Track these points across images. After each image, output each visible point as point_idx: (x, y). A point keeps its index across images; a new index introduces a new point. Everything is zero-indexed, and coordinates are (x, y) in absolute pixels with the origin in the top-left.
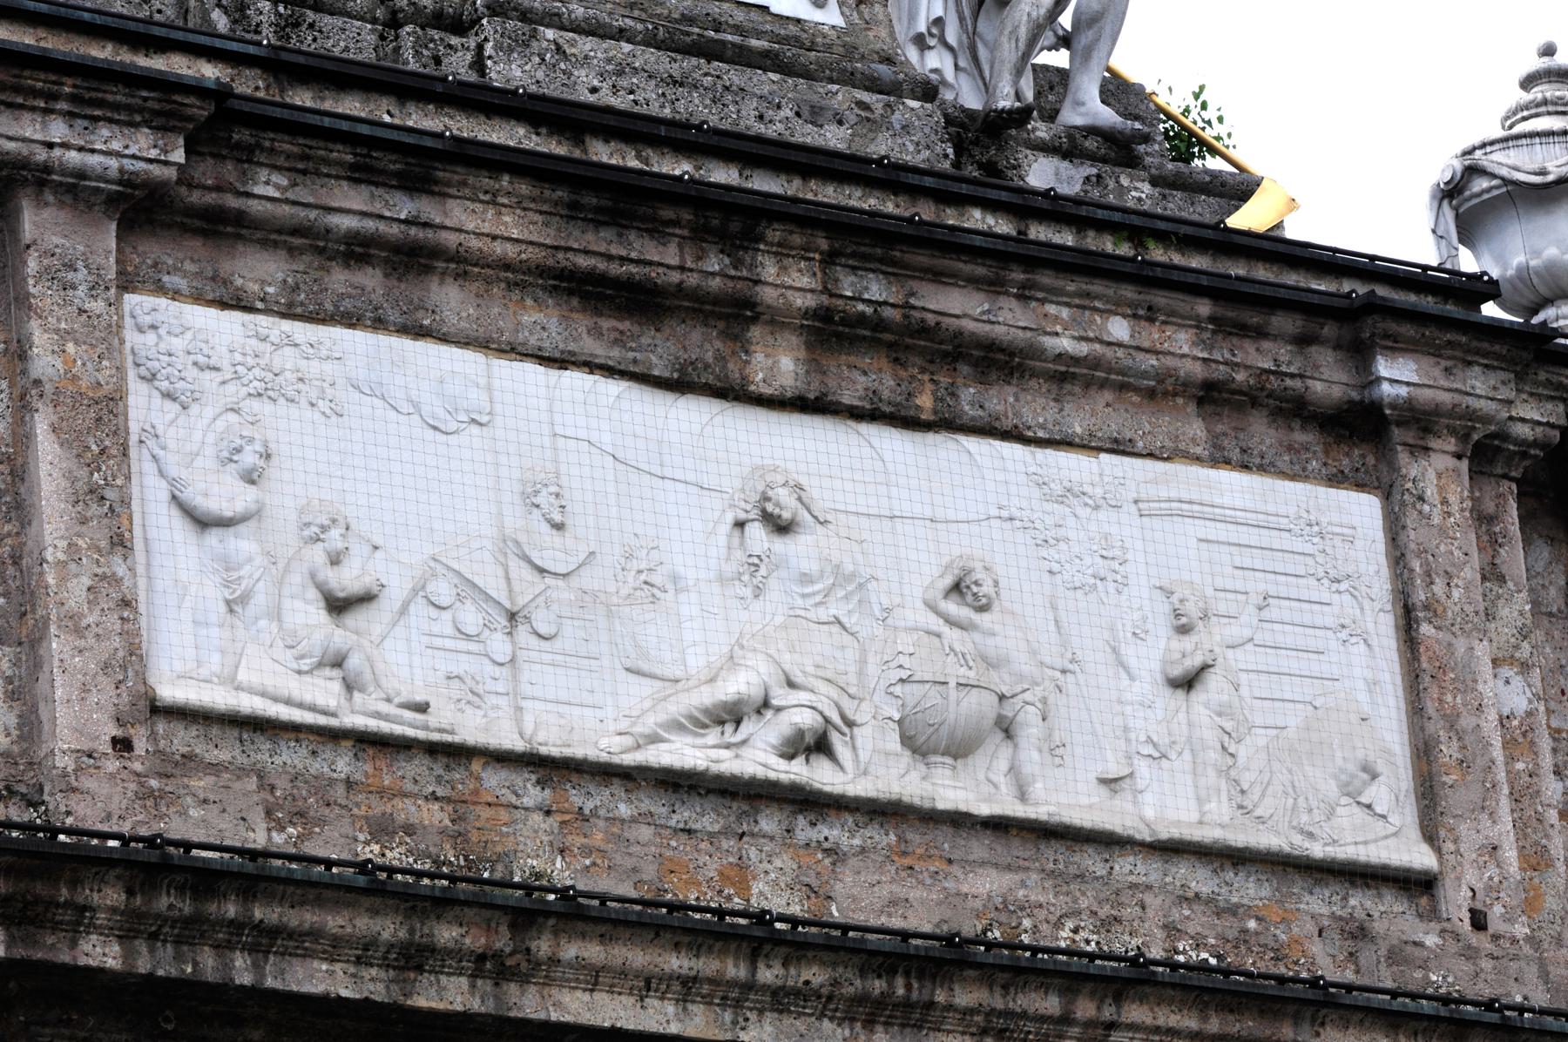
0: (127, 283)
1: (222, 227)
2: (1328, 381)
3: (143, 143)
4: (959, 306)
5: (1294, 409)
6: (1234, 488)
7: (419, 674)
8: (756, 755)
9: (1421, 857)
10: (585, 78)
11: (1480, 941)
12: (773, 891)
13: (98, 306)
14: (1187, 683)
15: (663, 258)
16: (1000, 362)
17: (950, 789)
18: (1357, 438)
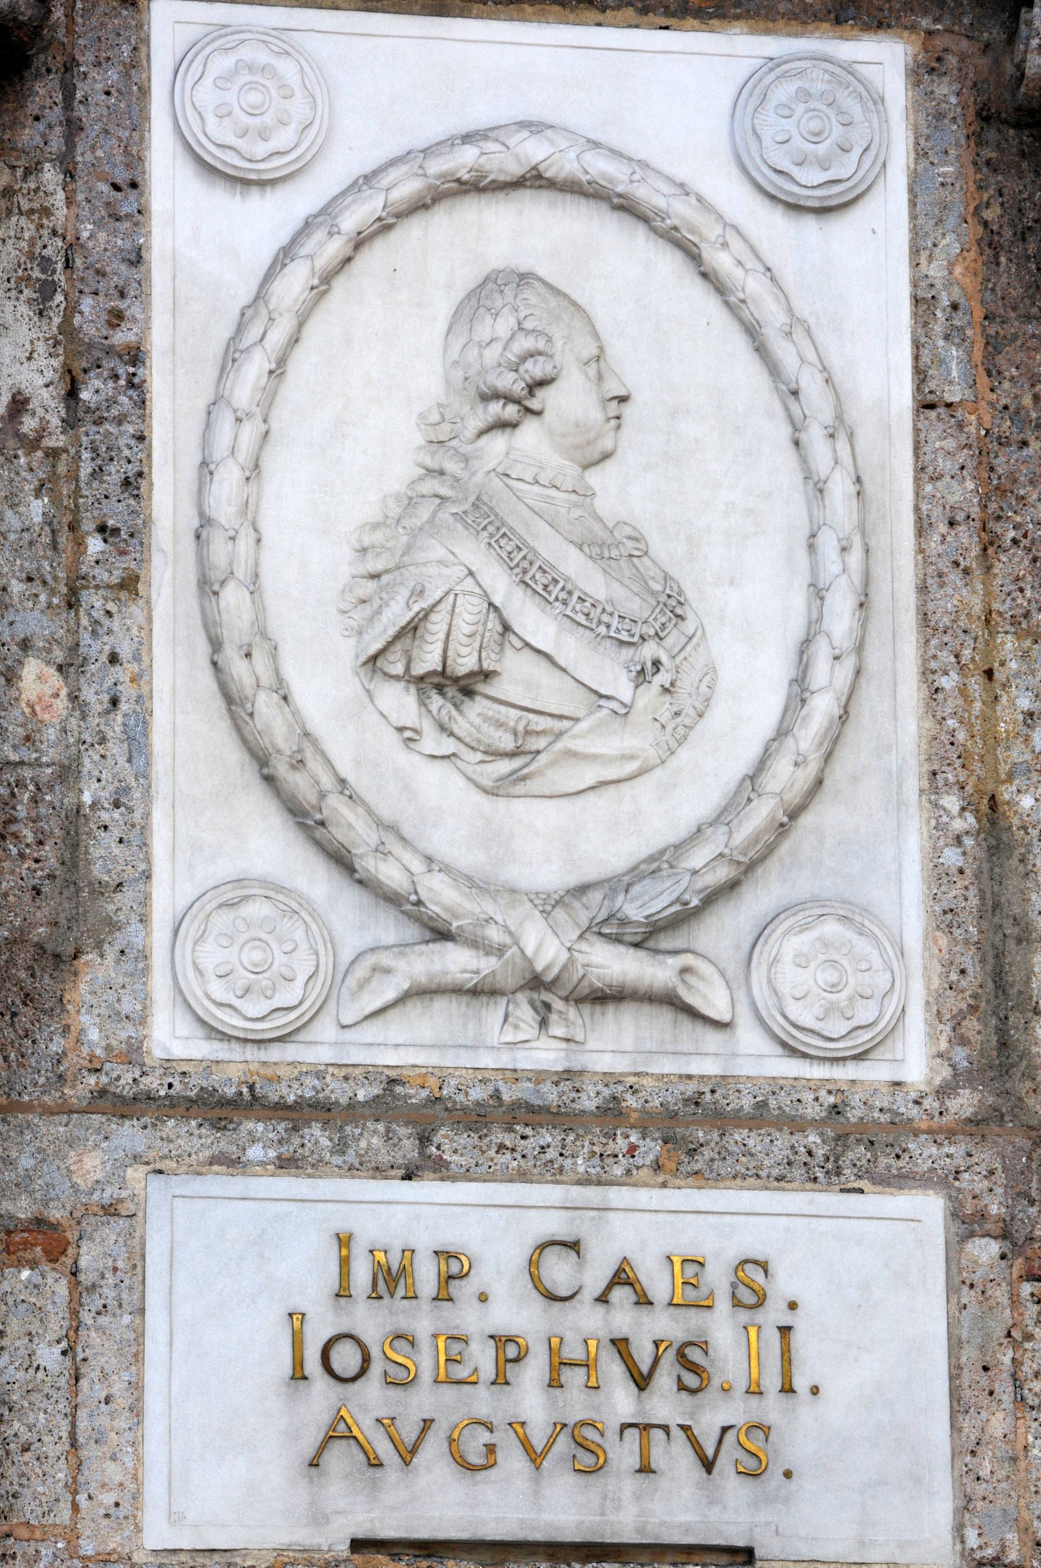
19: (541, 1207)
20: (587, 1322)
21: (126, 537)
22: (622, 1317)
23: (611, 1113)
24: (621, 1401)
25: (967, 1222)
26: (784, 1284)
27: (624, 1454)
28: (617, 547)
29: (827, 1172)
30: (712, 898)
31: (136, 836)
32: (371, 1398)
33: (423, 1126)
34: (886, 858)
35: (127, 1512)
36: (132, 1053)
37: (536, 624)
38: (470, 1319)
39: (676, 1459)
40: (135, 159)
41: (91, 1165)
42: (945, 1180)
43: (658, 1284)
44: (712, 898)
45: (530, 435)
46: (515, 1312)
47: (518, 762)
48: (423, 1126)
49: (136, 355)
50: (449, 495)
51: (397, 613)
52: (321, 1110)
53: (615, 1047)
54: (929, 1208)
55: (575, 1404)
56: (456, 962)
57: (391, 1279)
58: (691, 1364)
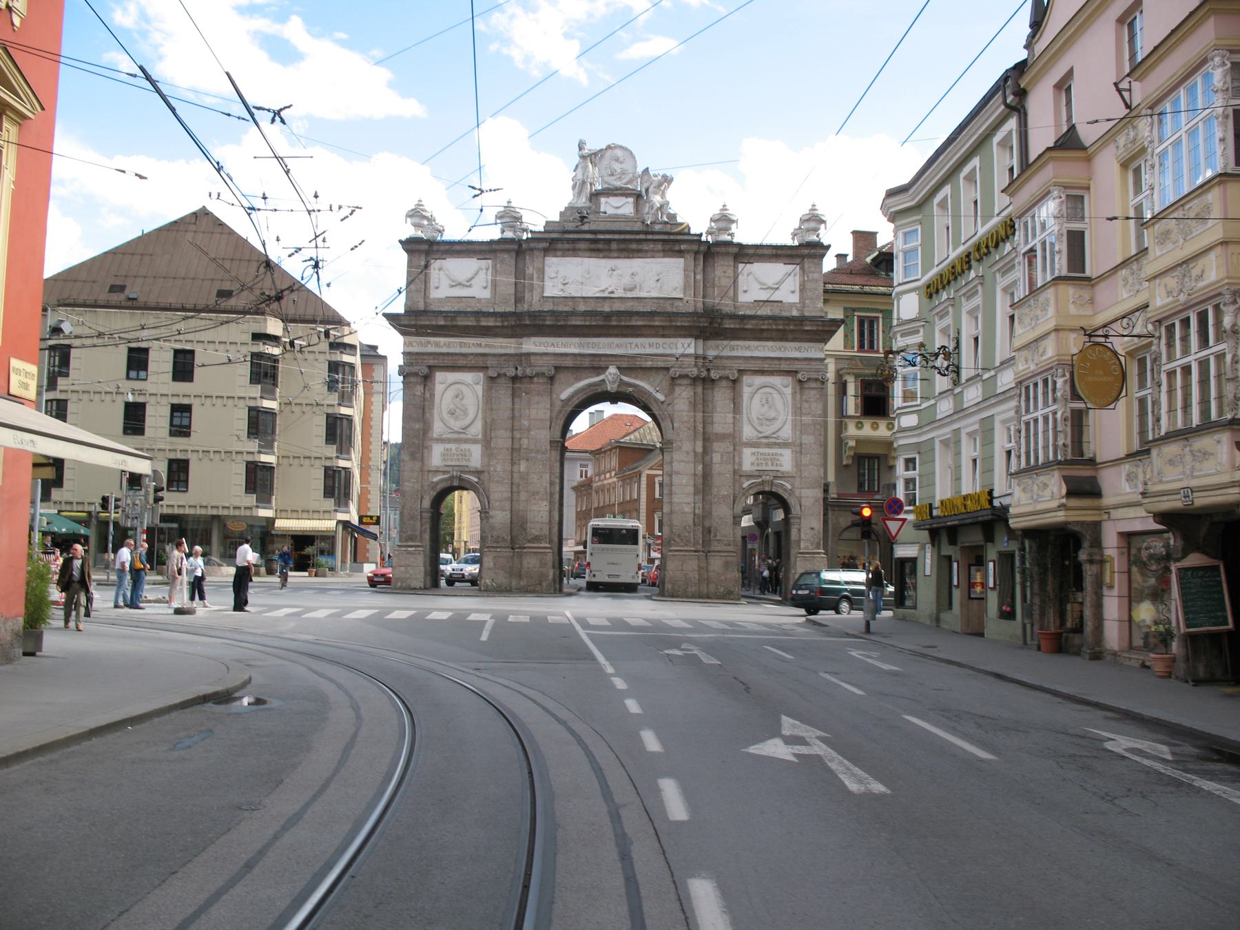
1: (556, 250)
2: (677, 248)
4: (634, 246)
5: (673, 251)
6: (666, 260)
7: (573, 291)
8: (606, 295)
9: (681, 296)
12: (607, 309)
15: (600, 246)
16: (639, 251)
17: (629, 295)
18: (680, 253)
47: (457, 419)
48: (449, 441)
53: (462, 436)
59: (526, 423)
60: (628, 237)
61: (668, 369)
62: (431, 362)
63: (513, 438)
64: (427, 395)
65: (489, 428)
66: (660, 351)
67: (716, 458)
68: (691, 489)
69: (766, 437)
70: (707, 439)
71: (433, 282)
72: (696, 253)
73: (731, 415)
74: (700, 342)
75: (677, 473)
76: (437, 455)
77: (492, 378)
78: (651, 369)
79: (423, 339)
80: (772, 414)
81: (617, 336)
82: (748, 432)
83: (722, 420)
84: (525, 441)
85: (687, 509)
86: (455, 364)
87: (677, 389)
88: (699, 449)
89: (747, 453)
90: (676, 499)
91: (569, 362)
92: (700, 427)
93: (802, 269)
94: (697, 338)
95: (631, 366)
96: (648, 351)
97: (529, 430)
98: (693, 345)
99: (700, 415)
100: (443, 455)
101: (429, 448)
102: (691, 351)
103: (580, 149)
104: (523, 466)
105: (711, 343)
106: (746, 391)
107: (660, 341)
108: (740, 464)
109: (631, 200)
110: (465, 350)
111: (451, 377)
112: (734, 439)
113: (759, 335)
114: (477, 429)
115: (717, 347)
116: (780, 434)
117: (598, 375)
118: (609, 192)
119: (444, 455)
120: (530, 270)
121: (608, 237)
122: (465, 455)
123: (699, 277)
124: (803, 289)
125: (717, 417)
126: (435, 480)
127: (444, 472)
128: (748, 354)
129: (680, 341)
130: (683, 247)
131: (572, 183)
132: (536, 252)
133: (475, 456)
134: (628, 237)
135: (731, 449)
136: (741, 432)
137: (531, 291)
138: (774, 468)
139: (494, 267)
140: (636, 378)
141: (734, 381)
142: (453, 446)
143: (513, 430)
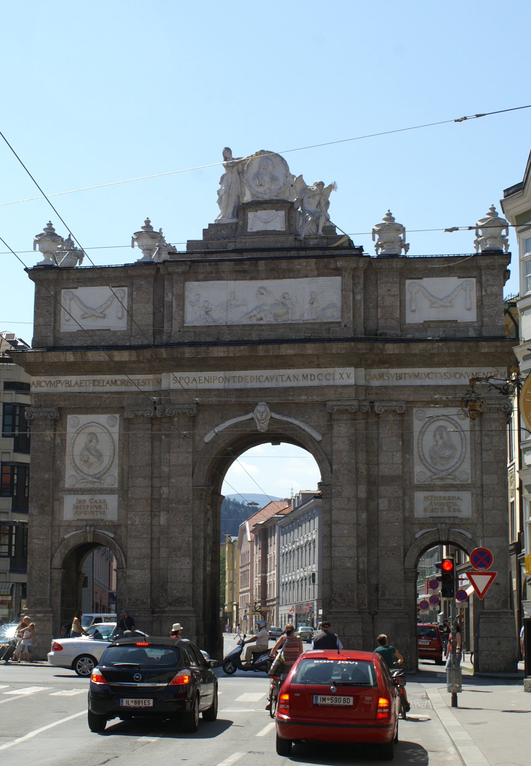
0: (185, 280)
2: (332, 266)
3: (184, 267)
4: (284, 264)
8: (254, 322)
10: (247, 244)
11: (346, 328)
13: (181, 285)
14: (312, 303)
16: (290, 270)
18: (337, 272)
19: (90, 497)
20: (93, 504)
21: (65, 452)
22: (96, 504)
23: (96, 490)
24: (95, 510)
25: (119, 497)
26: (107, 501)
27: (95, 513)
28: (97, 451)
29: (109, 494)
30: (103, 475)
31: (65, 473)
32: (78, 510)
33: (83, 491)
34: (115, 471)
35: (62, 518)
36: (64, 487)
37: (91, 457)
38: (86, 504)
39: (99, 513)
40: (66, 426)
41: (61, 495)
42: (118, 494)
43: (98, 501)
44: (103, 475)
45: (92, 443)
46: (88, 504)
48: (83, 491)
49: (66, 440)
50: (87, 448)
51: (82, 456)
52: (76, 490)
53: (96, 486)
54: (117, 496)
55: (92, 510)
56: (85, 480)
57: (80, 501)
58: (100, 507)
59: (166, 469)
60: (277, 254)
61: (324, 404)
62: (62, 404)
63: (152, 487)
64: (58, 440)
65: (126, 475)
66: (316, 383)
67: (383, 504)
68: (353, 541)
69: (442, 479)
70: (373, 482)
71: (63, 316)
72: (355, 269)
73: (399, 455)
74: (362, 371)
75: (337, 523)
76: (69, 509)
77: (129, 419)
78: (305, 404)
79: (53, 379)
80: (448, 453)
81: (266, 368)
82: (420, 473)
83: (389, 462)
84: (165, 490)
85: (349, 565)
86: (87, 404)
87: (335, 427)
88: (363, 495)
89: (419, 496)
90: (336, 554)
91: (214, 400)
92: (363, 469)
93: (480, 282)
94: (357, 366)
95: (283, 400)
96: (302, 383)
97: (169, 477)
98: (352, 375)
99: (362, 457)
100: (76, 507)
101: (60, 501)
102: (352, 382)
103: (226, 159)
104: (163, 519)
105: (375, 371)
106: (417, 425)
107: (315, 371)
108: (412, 510)
109: (282, 214)
110: (98, 389)
111: (84, 419)
112: (404, 483)
113: (429, 361)
114: (112, 480)
115: (381, 376)
116: (457, 473)
117: (246, 413)
118: (258, 204)
119: (77, 508)
120: (168, 298)
121: (255, 255)
122: (100, 507)
123: (359, 297)
124: (480, 306)
125: (383, 459)
126: (66, 537)
127: (77, 528)
128: (418, 382)
129: (339, 370)
130: (339, 264)
131: (217, 197)
132: (175, 277)
133: (111, 508)
134: (277, 254)
135: (400, 493)
136: (411, 473)
137: (171, 320)
138: (451, 514)
139: (130, 295)
140: (289, 416)
141: (402, 415)
142: (86, 497)
143: (152, 478)
